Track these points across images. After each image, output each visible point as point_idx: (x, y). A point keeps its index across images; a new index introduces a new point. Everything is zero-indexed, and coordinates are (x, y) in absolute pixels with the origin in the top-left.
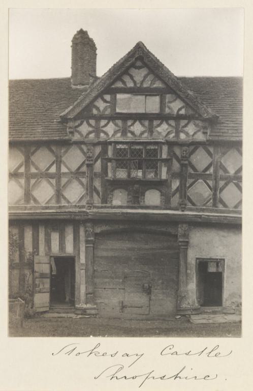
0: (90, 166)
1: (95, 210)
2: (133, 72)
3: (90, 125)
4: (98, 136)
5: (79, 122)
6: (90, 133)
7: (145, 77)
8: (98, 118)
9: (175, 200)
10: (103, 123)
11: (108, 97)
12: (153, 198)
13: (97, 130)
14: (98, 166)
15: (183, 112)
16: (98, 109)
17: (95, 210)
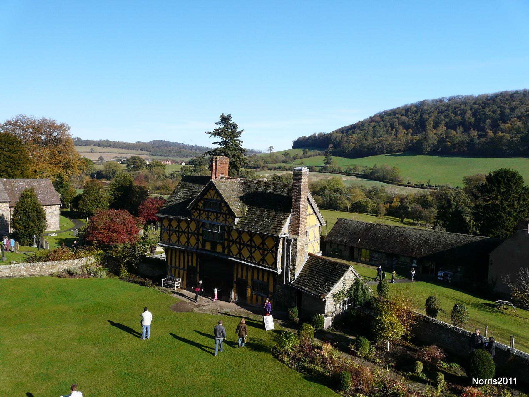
0: (198, 232)
1: (199, 251)
2: (210, 191)
3: (197, 213)
4: (200, 218)
5: (194, 211)
6: (198, 216)
7: (215, 194)
8: (200, 210)
9: (226, 251)
10: (202, 212)
11: (202, 202)
12: (219, 249)
13: (200, 216)
14: (201, 232)
15: (227, 212)
16: (199, 206)
17: (199, 251)
